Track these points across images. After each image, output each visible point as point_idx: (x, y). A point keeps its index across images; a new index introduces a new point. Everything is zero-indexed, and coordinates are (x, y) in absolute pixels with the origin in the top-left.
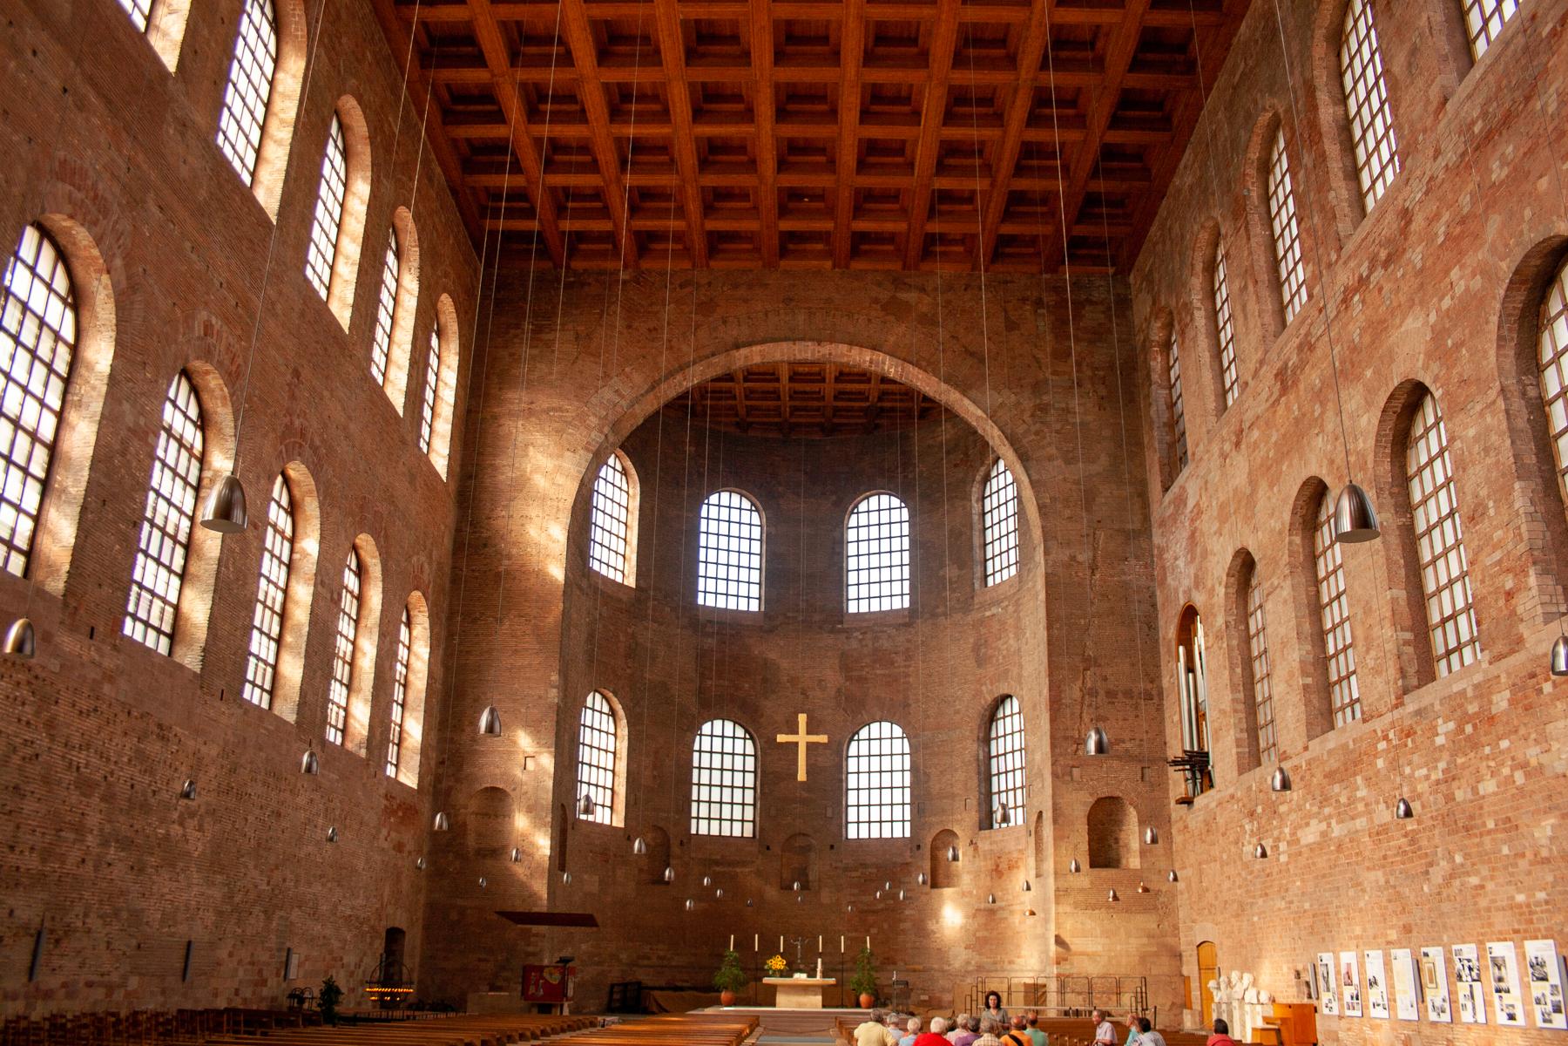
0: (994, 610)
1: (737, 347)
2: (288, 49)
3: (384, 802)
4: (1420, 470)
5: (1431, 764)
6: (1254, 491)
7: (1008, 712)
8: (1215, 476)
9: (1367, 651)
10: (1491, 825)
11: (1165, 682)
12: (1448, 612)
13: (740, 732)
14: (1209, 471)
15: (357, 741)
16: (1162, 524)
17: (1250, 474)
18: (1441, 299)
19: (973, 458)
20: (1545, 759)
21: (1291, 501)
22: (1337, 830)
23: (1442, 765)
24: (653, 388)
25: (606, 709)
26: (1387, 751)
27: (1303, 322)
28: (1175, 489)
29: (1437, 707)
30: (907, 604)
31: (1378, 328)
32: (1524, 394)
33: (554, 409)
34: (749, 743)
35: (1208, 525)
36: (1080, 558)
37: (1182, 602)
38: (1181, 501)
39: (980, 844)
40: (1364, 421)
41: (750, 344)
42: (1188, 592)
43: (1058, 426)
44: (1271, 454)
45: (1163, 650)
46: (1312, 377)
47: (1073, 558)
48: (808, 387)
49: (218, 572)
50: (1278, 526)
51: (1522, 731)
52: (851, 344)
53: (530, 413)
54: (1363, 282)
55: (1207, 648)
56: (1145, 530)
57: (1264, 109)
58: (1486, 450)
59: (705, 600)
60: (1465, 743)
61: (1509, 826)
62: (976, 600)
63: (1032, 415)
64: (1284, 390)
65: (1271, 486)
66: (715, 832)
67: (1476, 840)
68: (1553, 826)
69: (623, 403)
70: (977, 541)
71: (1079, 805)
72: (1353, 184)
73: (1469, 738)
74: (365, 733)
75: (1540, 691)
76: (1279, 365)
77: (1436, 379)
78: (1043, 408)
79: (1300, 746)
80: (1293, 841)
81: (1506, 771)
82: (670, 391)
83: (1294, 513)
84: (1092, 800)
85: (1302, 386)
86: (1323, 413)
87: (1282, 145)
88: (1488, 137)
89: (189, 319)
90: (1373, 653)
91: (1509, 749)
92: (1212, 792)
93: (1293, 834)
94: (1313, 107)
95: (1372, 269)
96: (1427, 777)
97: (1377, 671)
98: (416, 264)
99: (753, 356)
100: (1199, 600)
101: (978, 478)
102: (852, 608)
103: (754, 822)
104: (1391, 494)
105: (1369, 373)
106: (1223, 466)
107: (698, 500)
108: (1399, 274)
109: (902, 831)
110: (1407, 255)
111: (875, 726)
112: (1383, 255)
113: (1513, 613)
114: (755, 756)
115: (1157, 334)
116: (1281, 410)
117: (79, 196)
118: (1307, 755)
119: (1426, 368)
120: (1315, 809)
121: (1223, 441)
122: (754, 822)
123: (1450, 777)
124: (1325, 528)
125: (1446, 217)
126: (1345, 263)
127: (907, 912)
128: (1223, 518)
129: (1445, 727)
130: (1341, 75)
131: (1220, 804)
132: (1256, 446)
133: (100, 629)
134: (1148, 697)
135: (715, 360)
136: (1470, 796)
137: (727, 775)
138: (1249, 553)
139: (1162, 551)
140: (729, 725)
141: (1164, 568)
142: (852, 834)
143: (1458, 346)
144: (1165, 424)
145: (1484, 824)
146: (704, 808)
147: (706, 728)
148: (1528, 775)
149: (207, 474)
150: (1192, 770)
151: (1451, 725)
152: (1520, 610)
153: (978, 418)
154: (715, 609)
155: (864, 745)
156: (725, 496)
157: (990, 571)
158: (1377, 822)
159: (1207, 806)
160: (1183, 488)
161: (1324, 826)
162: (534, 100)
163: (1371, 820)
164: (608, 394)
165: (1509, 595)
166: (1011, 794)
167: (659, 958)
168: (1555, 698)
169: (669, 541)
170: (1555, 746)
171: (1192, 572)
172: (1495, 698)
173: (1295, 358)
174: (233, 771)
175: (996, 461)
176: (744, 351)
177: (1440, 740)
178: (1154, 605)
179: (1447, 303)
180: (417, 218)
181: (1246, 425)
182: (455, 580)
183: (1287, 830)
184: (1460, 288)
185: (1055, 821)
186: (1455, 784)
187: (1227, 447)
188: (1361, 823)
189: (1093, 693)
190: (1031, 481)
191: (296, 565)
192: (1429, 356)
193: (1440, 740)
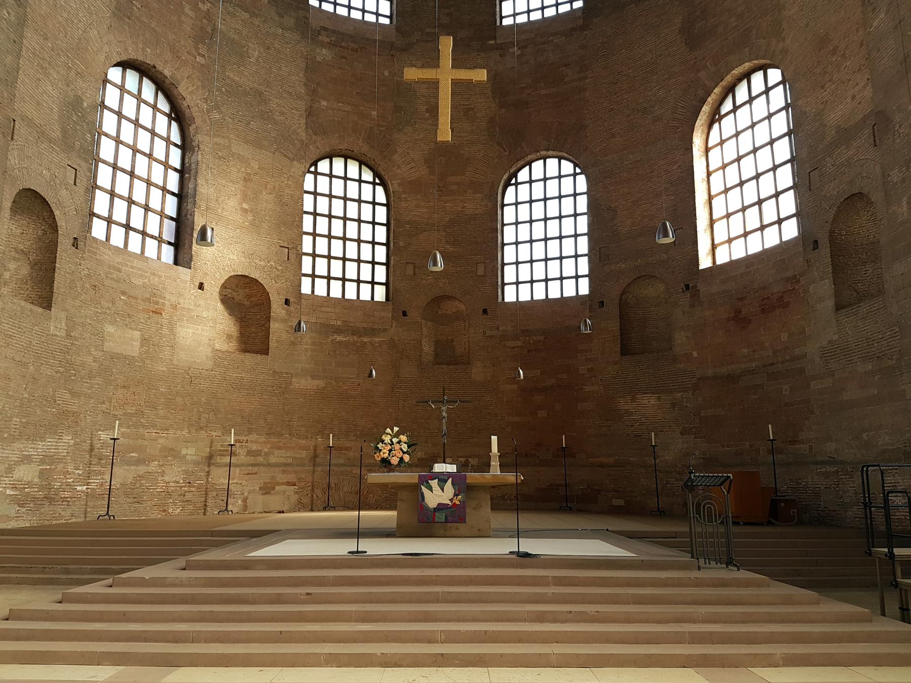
13: (368, 176)
34: (380, 190)
103: (387, 284)
111: (538, 166)
127: (587, 389)
155: (523, 190)
167: (250, 453)
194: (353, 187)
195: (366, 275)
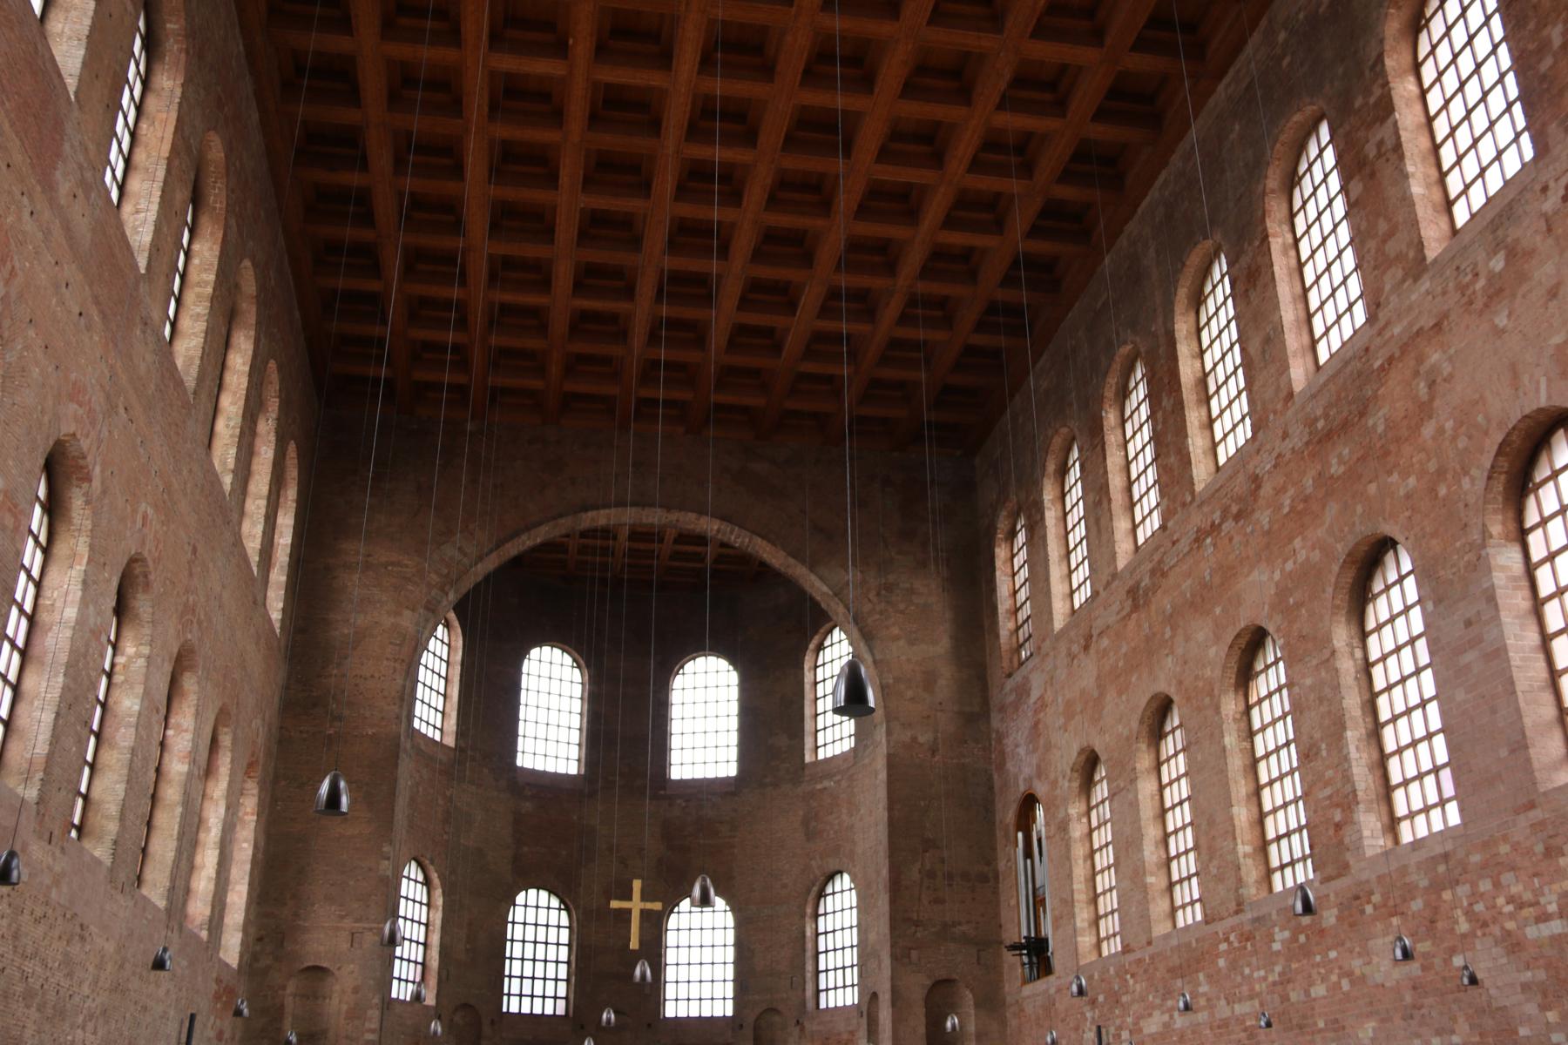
0: (826, 783)
1: (585, 509)
2: (205, 220)
3: (215, 986)
4: (1260, 701)
5: (1269, 966)
6: (1102, 695)
7: (837, 888)
8: (1062, 674)
9: (1210, 860)
10: (1321, 1024)
11: (1002, 865)
12: (1282, 830)
13: (555, 902)
14: (1055, 668)
15: (198, 922)
16: (1002, 709)
17: (1098, 677)
18: (1285, 561)
19: (809, 624)
20: (1367, 970)
21: (1140, 712)
22: (1180, 1021)
23: (1278, 969)
24: (498, 547)
25: (420, 878)
26: (1227, 952)
27: (1157, 549)
28: (1018, 677)
29: (1274, 917)
30: (732, 770)
31: (1228, 573)
32: (1352, 654)
33: (392, 564)
34: (564, 914)
35: (1052, 718)
36: (921, 739)
37: (1022, 788)
38: (1023, 690)
39: (807, 1025)
40: (1212, 651)
41: (596, 507)
42: (1029, 780)
43: (902, 606)
44: (1121, 664)
45: (999, 834)
46: (1164, 602)
47: (914, 739)
48: (642, 546)
49: (131, 761)
50: (1126, 732)
51: (1348, 944)
52: (702, 512)
53: (368, 567)
54: (1214, 528)
55: (1048, 837)
56: (984, 712)
57: (1125, 343)
58: (1321, 700)
59: (524, 761)
60: (1295, 951)
61: (1337, 1026)
62: (807, 772)
63: (878, 594)
64: (1136, 607)
65: (1120, 693)
66: (526, 1010)
67: (1309, 1038)
68: (1374, 1030)
69: (466, 561)
70: (808, 711)
71: (917, 986)
72: (1208, 433)
73: (1301, 947)
74: (208, 912)
75: (1363, 912)
76: (1131, 583)
77: (1278, 630)
78: (889, 588)
79: (1144, 942)
80: (1136, 1030)
81: (1334, 978)
82: (513, 549)
83: (1141, 722)
84: (929, 983)
85: (1153, 607)
86: (1172, 637)
87: (1139, 375)
88: (1328, 436)
89: (135, 511)
90: (1215, 862)
91: (1336, 959)
92: (1051, 978)
93: (1136, 1023)
94: (1173, 357)
95: (1224, 519)
96: (1265, 979)
97: (1220, 879)
98: (274, 416)
99: (601, 518)
100: (1041, 789)
101: (812, 646)
102: (676, 773)
103: (567, 998)
104: (1235, 719)
105: (1218, 610)
106: (1070, 665)
107: (522, 653)
108: (1249, 530)
109: (725, 1009)
110: (1257, 515)
112: (1234, 509)
113: (1341, 842)
114: (570, 927)
115: (1002, 525)
116: (1132, 624)
117: (81, 411)
118: (1151, 950)
119: (1270, 617)
120: (1158, 1001)
121: (1071, 641)
122: (567, 998)
123: (1286, 980)
124: (1170, 738)
125: (1291, 492)
126: (1200, 506)
128: (1069, 714)
129: (1281, 935)
130: (1199, 330)
131: (1059, 990)
132: (1105, 653)
133: (56, 833)
134: (984, 879)
135: (562, 521)
136: (1302, 997)
137: (529, 947)
138: (1093, 751)
139: (1001, 737)
140: (544, 894)
141: (1002, 753)
142: (670, 1011)
143: (1299, 605)
144: (1008, 611)
145: (1315, 1024)
146: (516, 982)
147: (520, 898)
148: (1352, 983)
149: (120, 660)
150: (1028, 955)
151: (1287, 934)
152: (1347, 840)
153: (824, 594)
154: (533, 772)
156: (546, 649)
157: (820, 742)
158: (1218, 1016)
159: (1047, 991)
160: (1026, 678)
161: (1166, 1017)
162: (415, 259)
163: (1212, 1015)
164: (450, 551)
165: (1338, 827)
166: (840, 972)
168: (1375, 919)
169: (490, 700)
170: (1375, 960)
171: (1034, 762)
172: (1325, 914)
173: (1146, 581)
174: (122, 967)
175: (830, 631)
176: (590, 514)
177: (1276, 946)
178: (991, 788)
179: (1289, 566)
180: (280, 368)
181: (1095, 632)
182: (280, 742)
183: (1129, 1020)
184: (1302, 556)
185: (894, 1004)
186: (1290, 986)
187: (1075, 648)
188: (1202, 1017)
189: (931, 875)
190: (875, 662)
191: (170, 741)
192: (1273, 607)
193: (1276, 946)
194: (542, 913)
195: (550, 992)
